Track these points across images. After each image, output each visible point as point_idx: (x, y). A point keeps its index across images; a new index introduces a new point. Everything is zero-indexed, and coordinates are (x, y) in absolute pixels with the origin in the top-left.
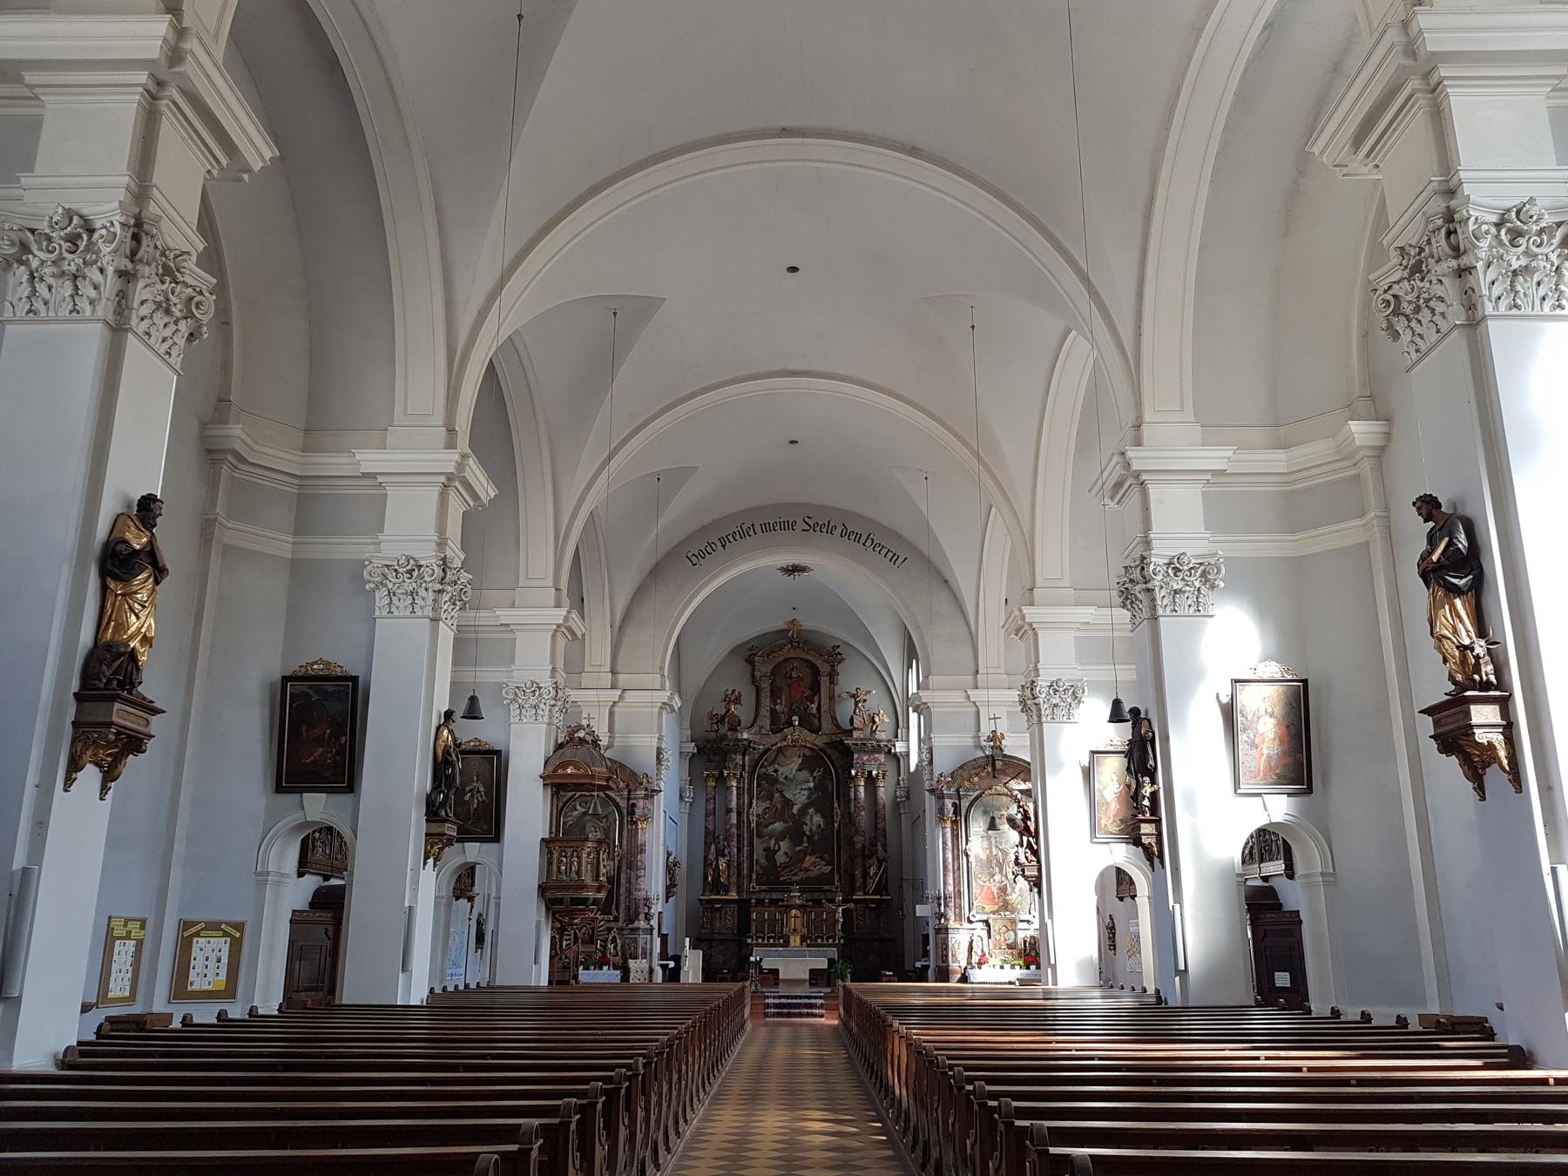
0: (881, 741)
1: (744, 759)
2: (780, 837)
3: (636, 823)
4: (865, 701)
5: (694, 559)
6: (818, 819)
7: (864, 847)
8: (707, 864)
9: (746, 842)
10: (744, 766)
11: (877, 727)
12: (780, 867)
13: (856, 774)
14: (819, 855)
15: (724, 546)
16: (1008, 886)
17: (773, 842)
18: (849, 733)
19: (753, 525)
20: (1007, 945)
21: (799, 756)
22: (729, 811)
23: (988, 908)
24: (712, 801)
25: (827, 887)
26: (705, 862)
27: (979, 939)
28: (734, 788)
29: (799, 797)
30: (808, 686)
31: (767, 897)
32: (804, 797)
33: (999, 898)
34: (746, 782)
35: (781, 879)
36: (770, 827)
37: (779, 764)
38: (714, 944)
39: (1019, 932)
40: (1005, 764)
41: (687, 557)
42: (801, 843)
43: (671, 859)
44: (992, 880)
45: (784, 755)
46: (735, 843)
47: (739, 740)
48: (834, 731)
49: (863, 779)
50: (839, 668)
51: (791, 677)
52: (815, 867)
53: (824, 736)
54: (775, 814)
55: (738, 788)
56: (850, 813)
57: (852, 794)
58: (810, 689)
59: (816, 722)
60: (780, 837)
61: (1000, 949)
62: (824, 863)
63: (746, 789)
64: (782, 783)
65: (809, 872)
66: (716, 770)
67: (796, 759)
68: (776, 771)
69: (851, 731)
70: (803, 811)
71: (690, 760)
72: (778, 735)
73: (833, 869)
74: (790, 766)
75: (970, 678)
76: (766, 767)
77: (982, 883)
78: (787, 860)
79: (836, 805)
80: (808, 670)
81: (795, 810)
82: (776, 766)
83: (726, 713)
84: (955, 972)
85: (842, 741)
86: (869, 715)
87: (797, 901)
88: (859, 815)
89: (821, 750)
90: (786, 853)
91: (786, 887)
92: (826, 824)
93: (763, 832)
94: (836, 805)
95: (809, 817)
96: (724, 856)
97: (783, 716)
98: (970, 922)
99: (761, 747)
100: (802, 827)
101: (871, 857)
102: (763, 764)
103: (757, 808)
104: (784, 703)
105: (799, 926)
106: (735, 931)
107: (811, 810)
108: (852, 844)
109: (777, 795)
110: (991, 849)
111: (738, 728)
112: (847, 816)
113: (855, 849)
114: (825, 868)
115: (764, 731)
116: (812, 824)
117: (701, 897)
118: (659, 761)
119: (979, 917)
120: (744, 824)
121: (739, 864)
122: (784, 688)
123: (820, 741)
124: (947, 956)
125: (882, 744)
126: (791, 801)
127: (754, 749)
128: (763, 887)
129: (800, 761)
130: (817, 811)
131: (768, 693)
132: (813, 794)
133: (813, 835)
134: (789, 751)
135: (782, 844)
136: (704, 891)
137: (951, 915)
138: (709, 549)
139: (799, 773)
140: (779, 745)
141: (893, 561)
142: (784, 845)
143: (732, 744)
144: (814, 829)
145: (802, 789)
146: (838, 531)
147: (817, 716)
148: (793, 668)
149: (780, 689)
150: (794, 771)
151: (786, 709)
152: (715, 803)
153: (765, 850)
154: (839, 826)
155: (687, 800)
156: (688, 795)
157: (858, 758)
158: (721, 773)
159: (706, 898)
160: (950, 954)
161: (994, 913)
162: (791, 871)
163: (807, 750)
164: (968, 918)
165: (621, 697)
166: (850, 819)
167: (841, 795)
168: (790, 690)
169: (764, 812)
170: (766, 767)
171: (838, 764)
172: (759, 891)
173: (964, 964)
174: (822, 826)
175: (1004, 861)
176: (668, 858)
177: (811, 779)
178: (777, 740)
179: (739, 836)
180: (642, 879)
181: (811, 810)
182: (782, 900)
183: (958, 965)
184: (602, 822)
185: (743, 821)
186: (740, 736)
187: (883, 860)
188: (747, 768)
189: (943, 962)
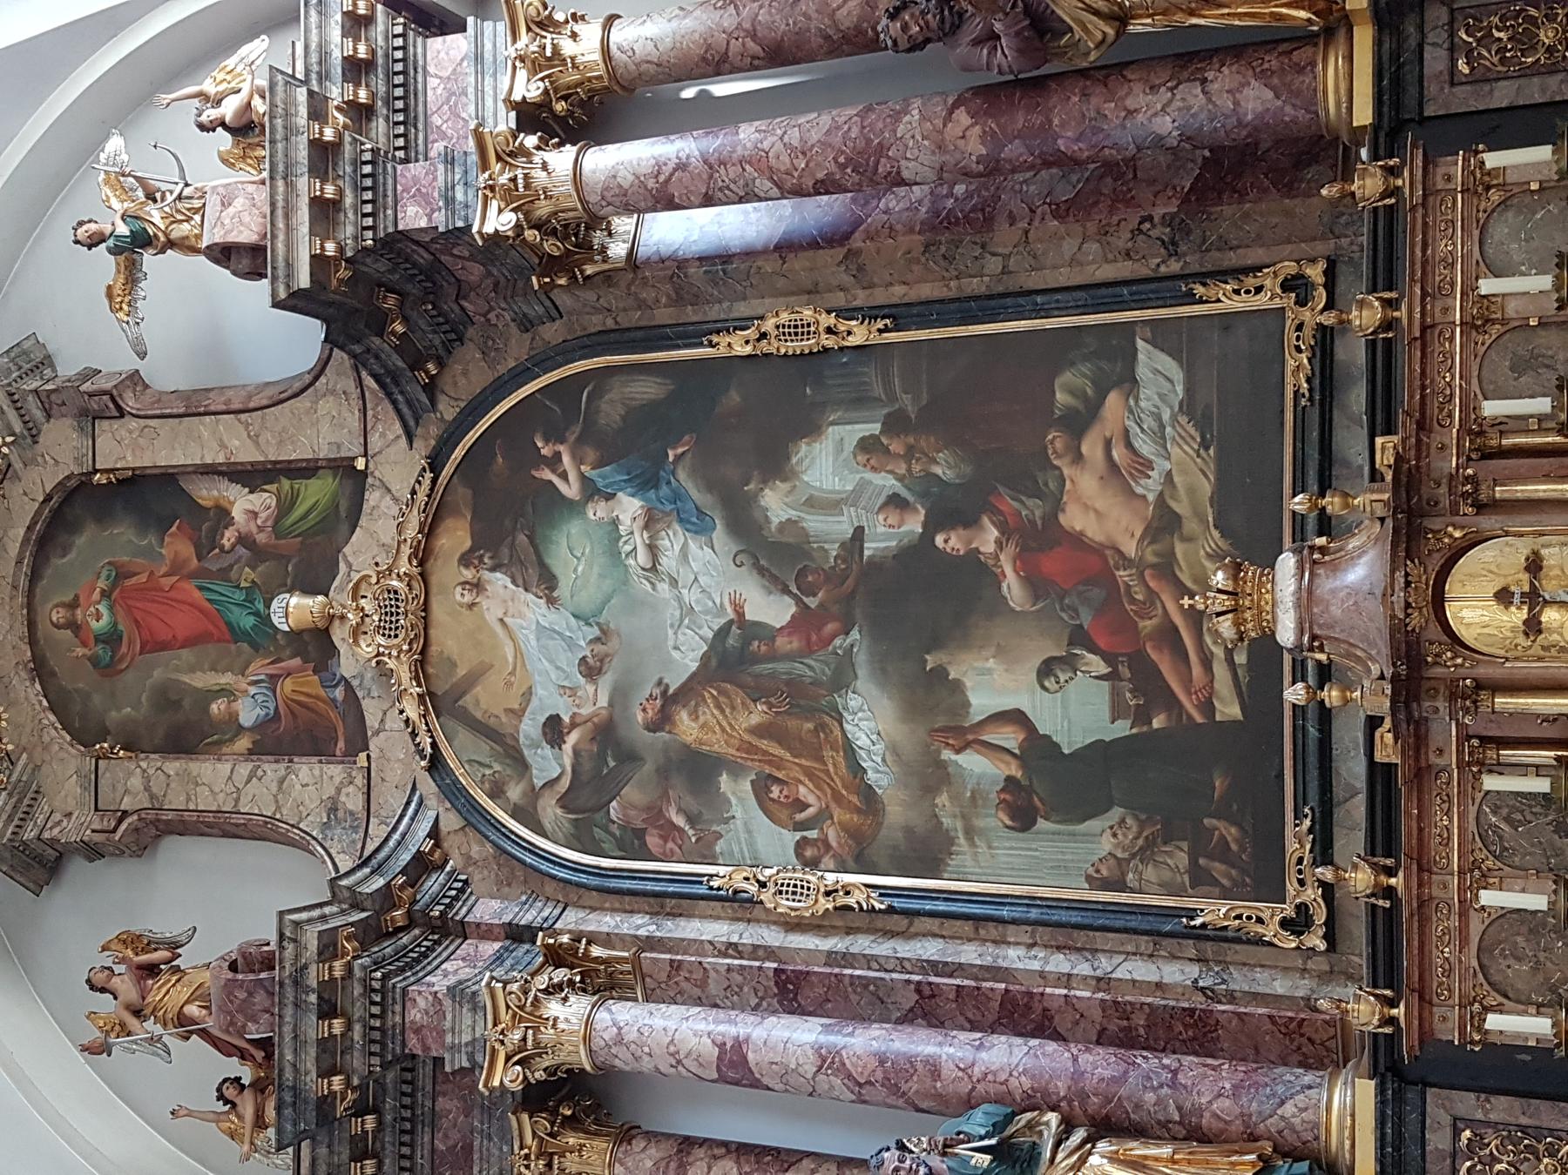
1: (485, 932)
9: (970, 954)
10: (517, 934)
12: (1142, 716)
14: (1056, 440)
17: (973, 763)
21: (477, 586)
25: (1297, 367)
28: (602, 1016)
30: (152, 539)
32: (700, 553)
34: (606, 922)
35: (1228, 709)
36: (871, 776)
37: (518, 714)
42: (978, 571)
48: (351, 385)
51: (111, 639)
52: (1143, 466)
53: (375, 441)
56: (785, 248)
58: (163, 526)
59: (317, 492)
62: (1113, 399)
64: (620, 695)
65: (1181, 507)
67: (491, 609)
68: (554, 730)
72: (372, 721)
73: (1161, 335)
78: (1098, 665)
79: (738, 345)
80: (81, 541)
82: (530, 728)
89: (435, 463)
90: (1046, 670)
92: (859, 402)
93: (909, 831)
95: (814, 523)
97: (288, 685)
100: (875, 565)
104: (226, 679)
107: (775, 504)
109: (687, 727)
114: (1148, 397)
115: (353, 800)
116: (853, 499)
120: (847, 959)
122: (158, 674)
126: (723, 633)
127: (422, 865)
129: (499, 581)
130: (776, 465)
131: (173, 766)
132: (677, 496)
135: (982, 701)
139: (563, 591)
140: (412, 712)
144: (886, 482)
147: (286, 483)
148: (74, 626)
149: (168, 698)
150: (559, 619)
151: (260, 668)
153: (1023, 818)
154: (869, 314)
158: (535, 1098)
162: (1169, 636)
167: (691, 314)
168: (163, 646)
169: (786, 812)
170: (534, 794)
171: (517, 350)
174: (875, 428)
177: (597, 511)
178: (394, 722)
181: (775, 504)
185: (831, 958)
188: (528, 917)
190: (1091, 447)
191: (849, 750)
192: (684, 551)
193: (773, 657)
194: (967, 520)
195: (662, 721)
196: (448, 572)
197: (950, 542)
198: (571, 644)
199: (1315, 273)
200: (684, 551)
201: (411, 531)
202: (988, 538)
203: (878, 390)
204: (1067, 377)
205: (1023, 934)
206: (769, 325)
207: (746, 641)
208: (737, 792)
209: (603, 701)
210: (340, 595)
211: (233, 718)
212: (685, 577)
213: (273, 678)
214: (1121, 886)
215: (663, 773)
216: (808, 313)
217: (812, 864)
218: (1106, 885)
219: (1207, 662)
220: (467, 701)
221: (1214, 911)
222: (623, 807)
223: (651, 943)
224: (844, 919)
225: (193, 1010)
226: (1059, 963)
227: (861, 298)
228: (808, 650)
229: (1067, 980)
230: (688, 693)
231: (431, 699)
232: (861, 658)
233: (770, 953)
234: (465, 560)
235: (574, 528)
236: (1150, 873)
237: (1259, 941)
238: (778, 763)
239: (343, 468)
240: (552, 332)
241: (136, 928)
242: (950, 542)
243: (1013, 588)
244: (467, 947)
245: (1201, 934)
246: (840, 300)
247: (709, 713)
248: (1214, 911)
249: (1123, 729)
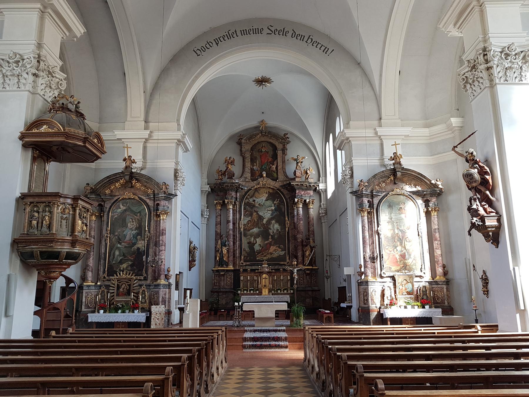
0: (311, 183)
1: (236, 195)
2: (257, 236)
3: (159, 216)
4: (302, 162)
5: (198, 52)
6: (277, 226)
7: (302, 241)
8: (216, 251)
9: (238, 239)
10: (236, 198)
11: (309, 176)
12: (257, 252)
13: (298, 201)
14: (278, 245)
15: (217, 44)
16: (406, 254)
17: (253, 239)
18: (294, 179)
19: (236, 31)
21: (266, 193)
22: (228, 222)
23: (394, 268)
24: (219, 217)
25: (282, 263)
26: (215, 250)
28: (231, 209)
29: (267, 214)
31: (249, 268)
33: (400, 262)
34: (238, 207)
35: (257, 259)
37: (255, 197)
38: (220, 294)
39: (415, 283)
40: (403, 174)
41: (194, 51)
42: (268, 239)
43: (192, 245)
44: (395, 250)
45: (258, 192)
46: (231, 239)
47: (233, 183)
49: (301, 204)
50: (288, 146)
54: (253, 224)
55: (233, 210)
56: (294, 223)
57: (296, 213)
60: (257, 236)
61: (403, 295)
63: (237, 211)
64: (257, 207)
66: (220, 200)
67: (265, 194)
68: (254, 201)
69: (295, 178)
70: (269, 221)
71: (207, 196)
73: (285, 253)
74: (262, 199)
75: (376, 123)
76: (248, 199)
77: (389, 252)
79: (287, 219)
81: (265, 221)
82: (254, 198)
83: (226, 170)
84: (373, 311)
85: (290, 183)
86: (304, 170)
87: (266, 270)
88: (300, 223)
90: (260, 245)
91: (260, 263)
92: (281, 229)
93: (247, 234)
94: (287, 219)
95: (272, 225)
96: (225, 246)
98: (381, 277)
99: (246, 188)
101: (306, 246)
102: (247, 197)
103: (244, 220)
105: (267, 284)
106: (232, 287)
107: (273, 222)
108: (295, 238)
109: (255, 214)
111: (233, 178)
112: (293, 224)
113: (297, 242)
116: (274, 229)
117: (213, 269)
118: (176, 177)
119: (388, 274)
120: (237, 229)
121: (234, 251)
123: (277, 185)
124: (367, 300)
125: (312, 185)
126: (263, 217)
127: (242, 189)
128: (248, 263)
129: (267, 195)
130: (276, 222)
132: (274, 213)
133: (274, 235)
134: (261, 190)
135: (257, 240)
136: (215, 266)
137: (369, 272)
138: (208, 46)
139: (266, 202)
140: (255, 187)
141: (325, 51)
142: (259, 240)
143: (229, 185)
144: (275, 232)
145: (268, 210)
146: (290, 34)
152: (221, 218)
153: (248, 243)
154: (288, 230)
155: (205, 216)
156: (206, 213)
157: (299, 193)
158: (224, 202)
159: (217, 269)
160: (370, 299)
161: (398, 271)
163: (270, 190)
164: (381, 275)
165: (150, 135)
166: (295, 226)
167: (289, 214)
170: (248, 199)
171: (287, 197)
172: (246, 265)
173: (378, 305)
176: (190, 245)
177: (273, 205)
179: (234, 236)
180: (163, 252)
181: (273, 222)
182: (258, 270)
183: (375, 306)
184: (137, 216)
186: (234, 181)
187: (314, 247)
188: (238, 199)
189: (365, 304)
190: (277, 248)
191: (253, 229)
192: (269, 213)
193: (261, 221)
194: (272, 238)
195: (255, 211)
196: (268, 190)
197: (270, 237)
198: (262, 202)
199: (289, 264)
200: (269, 213)
201: (271, 187)
202: (270, 240)
203: (282, 231)
204: (283, 246)
205: (239, 243)
206: (288, 221)
207: (262, 219)
208: (249, 218)
209: (257, 206)
210: (266, 179)
211: (254, 166)
212: (267, 213)
213: (258, 170)
214: (244, 251)
215: (251, 211)
216: (289, 225)
217: (244, 225)
218: (244, 249)
219: (261, 257)
220: (256, 192)
221: (243, 257)
222: (248, 208)
223: (236, 211)
224: (240, 228)
225: (229, 169)
226: (238, 246)
227: (290, 229)
228: (261, 225)
229: (237, 247)
230: (258, 214)
231: (257, 188)
232: (261, 229)
233: (236, 222)
234: (269, 192)
235: (272, 203)
236: (245, 253)
237: (240, 261)
238: (252, 222)
239: (277, 179)
240: (288, 200)
241: (235, 161)
242: (270, 237)
243: (266, 242)
244: (235, 193)
245: (241, 256)
246: (290, 227)
247: (256, 216)
248: (243, 257)
249: (256, 251)
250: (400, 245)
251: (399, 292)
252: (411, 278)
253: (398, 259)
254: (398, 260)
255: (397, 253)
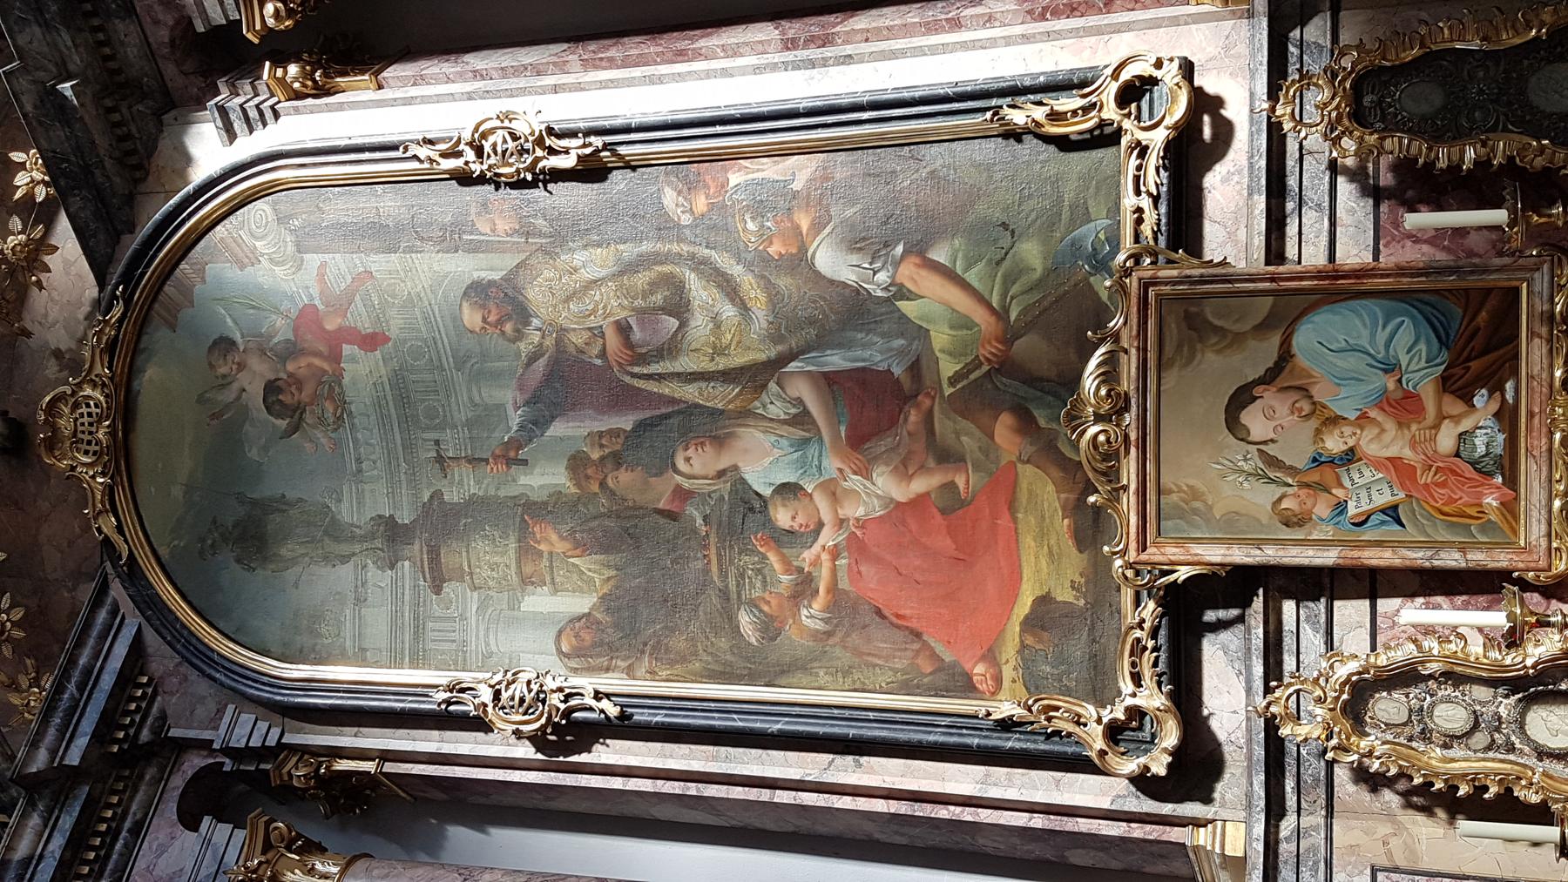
20: (1457, 386)
27: (1388, 707)
61: (1507, 467)
77: (812, 616)
110: (534, 510)
175: (622, 398)
250: (720, 441)
251: (1460, 519)
252: (1209, 311)
253: (901, 492)
254: (919, 485)
255: (833, 492)
